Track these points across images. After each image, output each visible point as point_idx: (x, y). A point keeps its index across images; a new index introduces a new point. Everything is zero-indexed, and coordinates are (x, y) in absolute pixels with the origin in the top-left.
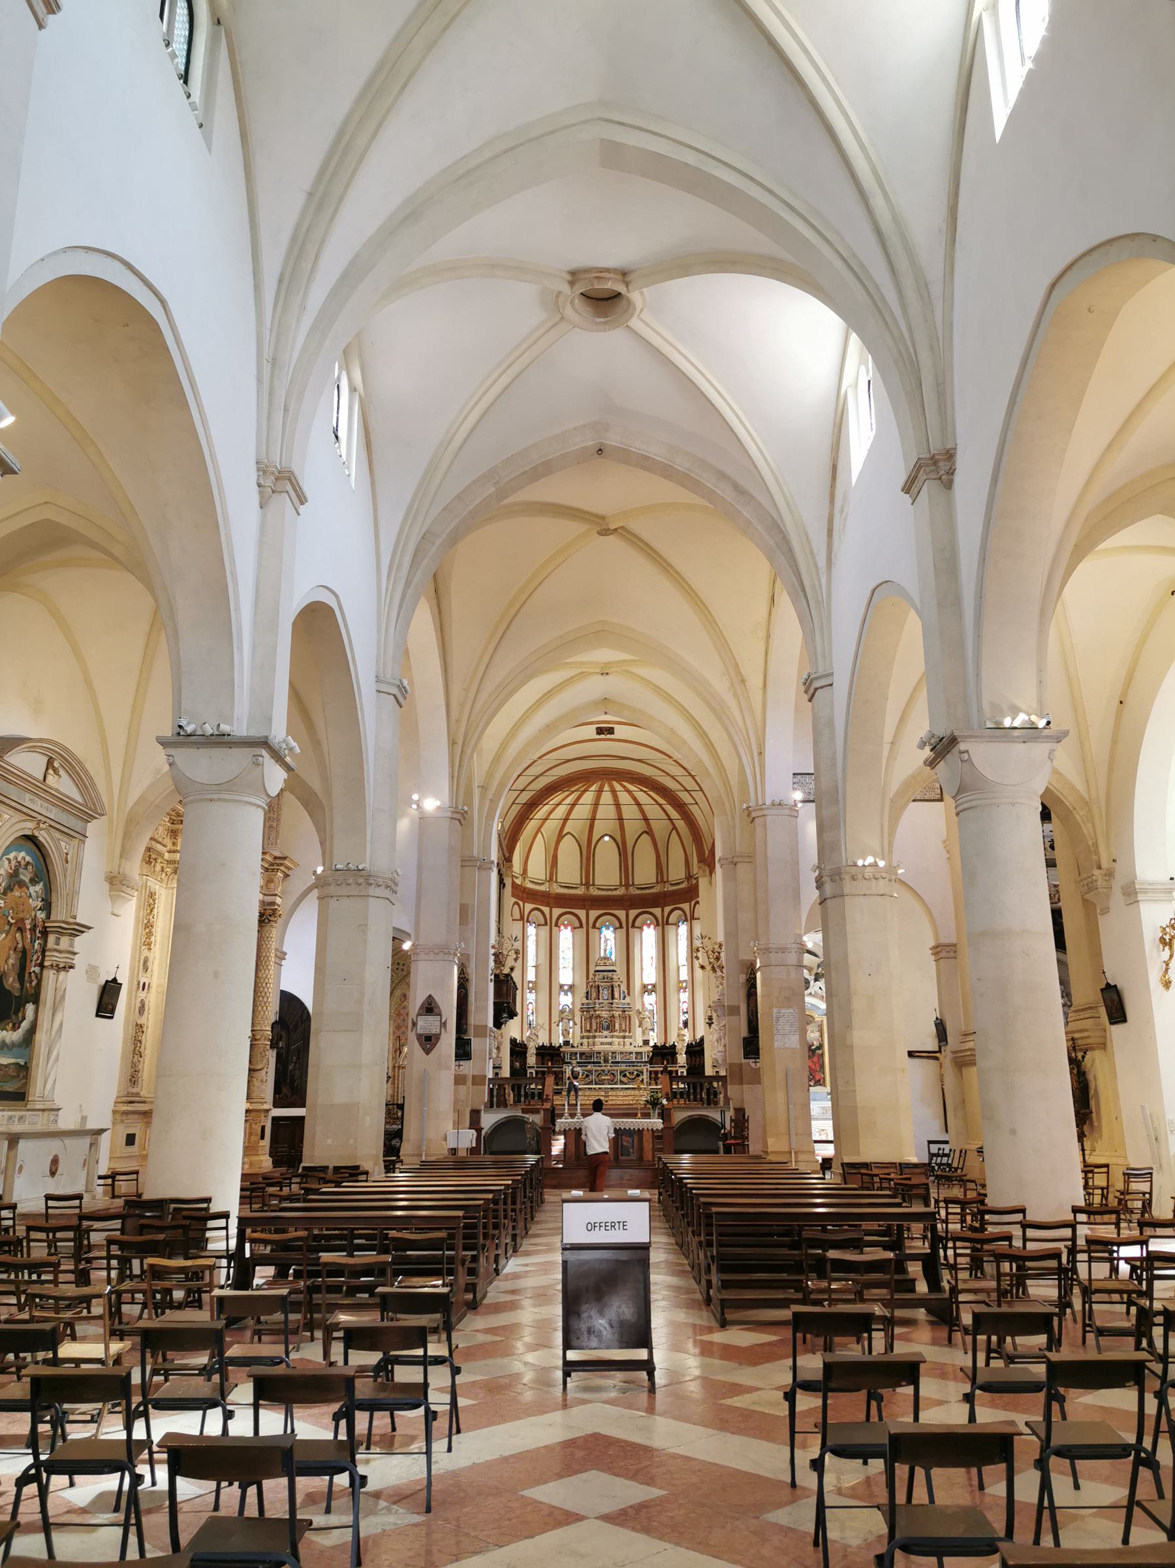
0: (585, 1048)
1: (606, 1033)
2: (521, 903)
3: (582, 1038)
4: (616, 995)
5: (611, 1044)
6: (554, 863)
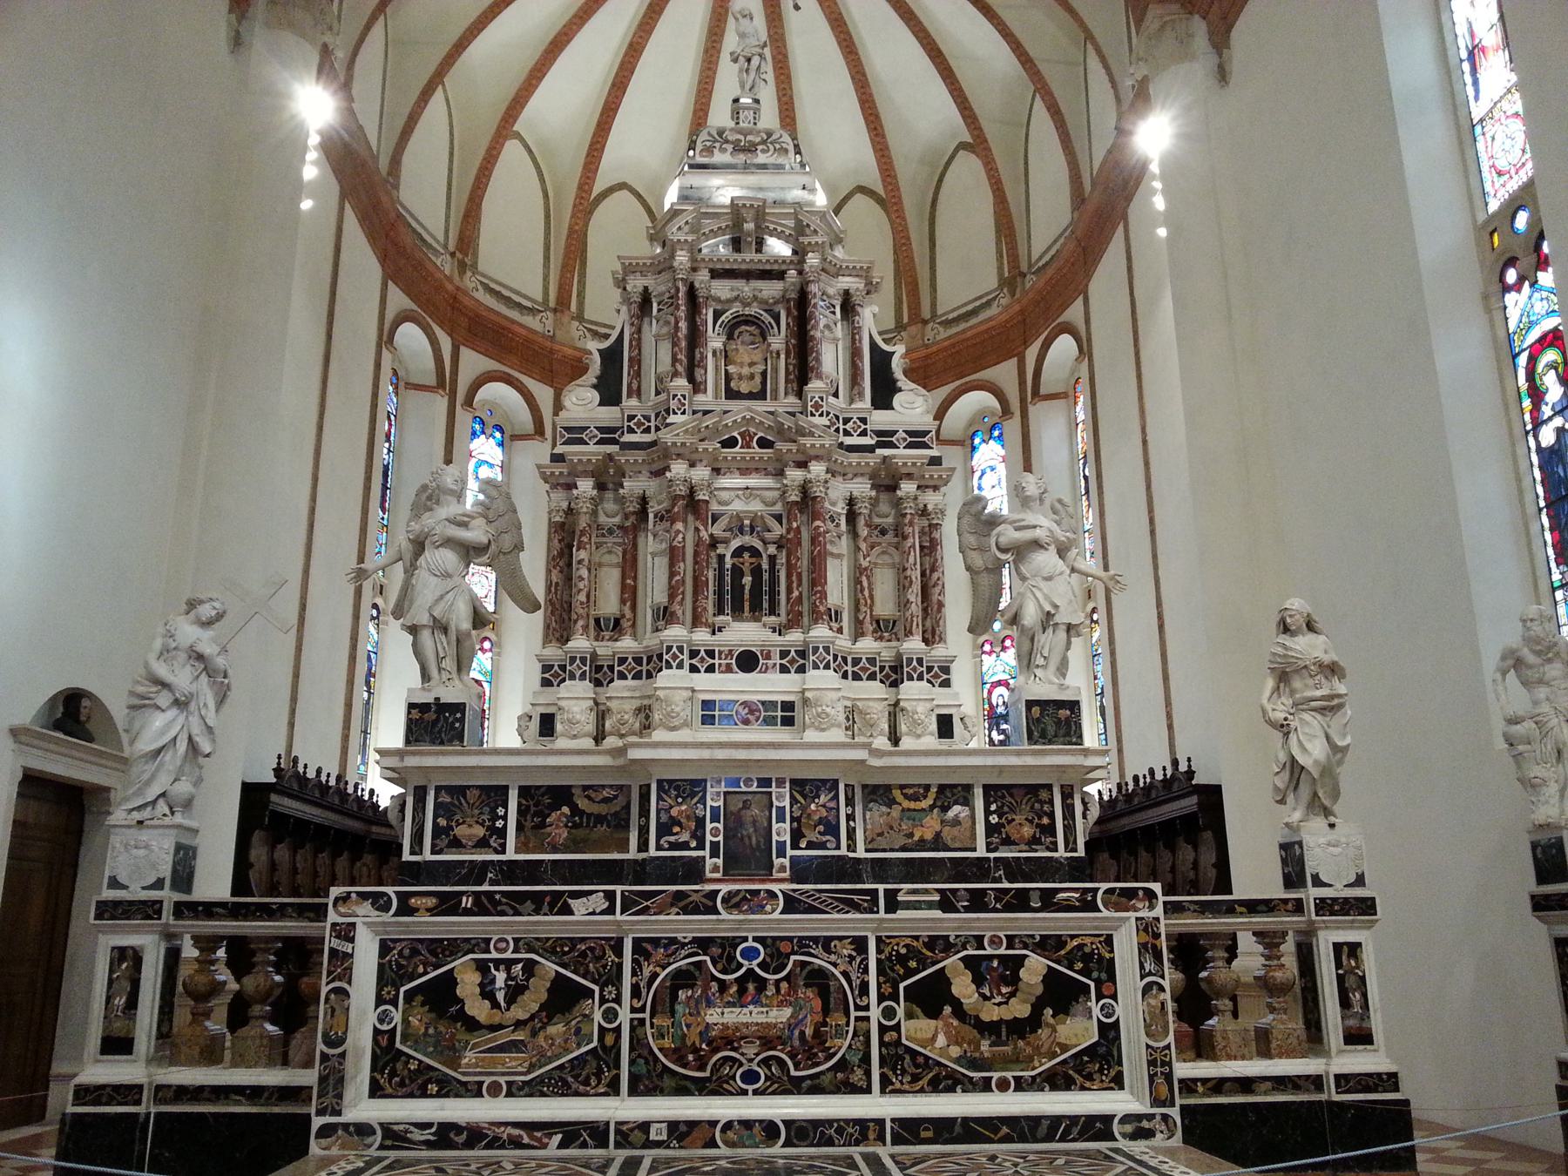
0: (573, 753)
1: (745, 633)
3: (551, 675)
4: (831, 358)
5: (787, 714)
6: (573, 254)
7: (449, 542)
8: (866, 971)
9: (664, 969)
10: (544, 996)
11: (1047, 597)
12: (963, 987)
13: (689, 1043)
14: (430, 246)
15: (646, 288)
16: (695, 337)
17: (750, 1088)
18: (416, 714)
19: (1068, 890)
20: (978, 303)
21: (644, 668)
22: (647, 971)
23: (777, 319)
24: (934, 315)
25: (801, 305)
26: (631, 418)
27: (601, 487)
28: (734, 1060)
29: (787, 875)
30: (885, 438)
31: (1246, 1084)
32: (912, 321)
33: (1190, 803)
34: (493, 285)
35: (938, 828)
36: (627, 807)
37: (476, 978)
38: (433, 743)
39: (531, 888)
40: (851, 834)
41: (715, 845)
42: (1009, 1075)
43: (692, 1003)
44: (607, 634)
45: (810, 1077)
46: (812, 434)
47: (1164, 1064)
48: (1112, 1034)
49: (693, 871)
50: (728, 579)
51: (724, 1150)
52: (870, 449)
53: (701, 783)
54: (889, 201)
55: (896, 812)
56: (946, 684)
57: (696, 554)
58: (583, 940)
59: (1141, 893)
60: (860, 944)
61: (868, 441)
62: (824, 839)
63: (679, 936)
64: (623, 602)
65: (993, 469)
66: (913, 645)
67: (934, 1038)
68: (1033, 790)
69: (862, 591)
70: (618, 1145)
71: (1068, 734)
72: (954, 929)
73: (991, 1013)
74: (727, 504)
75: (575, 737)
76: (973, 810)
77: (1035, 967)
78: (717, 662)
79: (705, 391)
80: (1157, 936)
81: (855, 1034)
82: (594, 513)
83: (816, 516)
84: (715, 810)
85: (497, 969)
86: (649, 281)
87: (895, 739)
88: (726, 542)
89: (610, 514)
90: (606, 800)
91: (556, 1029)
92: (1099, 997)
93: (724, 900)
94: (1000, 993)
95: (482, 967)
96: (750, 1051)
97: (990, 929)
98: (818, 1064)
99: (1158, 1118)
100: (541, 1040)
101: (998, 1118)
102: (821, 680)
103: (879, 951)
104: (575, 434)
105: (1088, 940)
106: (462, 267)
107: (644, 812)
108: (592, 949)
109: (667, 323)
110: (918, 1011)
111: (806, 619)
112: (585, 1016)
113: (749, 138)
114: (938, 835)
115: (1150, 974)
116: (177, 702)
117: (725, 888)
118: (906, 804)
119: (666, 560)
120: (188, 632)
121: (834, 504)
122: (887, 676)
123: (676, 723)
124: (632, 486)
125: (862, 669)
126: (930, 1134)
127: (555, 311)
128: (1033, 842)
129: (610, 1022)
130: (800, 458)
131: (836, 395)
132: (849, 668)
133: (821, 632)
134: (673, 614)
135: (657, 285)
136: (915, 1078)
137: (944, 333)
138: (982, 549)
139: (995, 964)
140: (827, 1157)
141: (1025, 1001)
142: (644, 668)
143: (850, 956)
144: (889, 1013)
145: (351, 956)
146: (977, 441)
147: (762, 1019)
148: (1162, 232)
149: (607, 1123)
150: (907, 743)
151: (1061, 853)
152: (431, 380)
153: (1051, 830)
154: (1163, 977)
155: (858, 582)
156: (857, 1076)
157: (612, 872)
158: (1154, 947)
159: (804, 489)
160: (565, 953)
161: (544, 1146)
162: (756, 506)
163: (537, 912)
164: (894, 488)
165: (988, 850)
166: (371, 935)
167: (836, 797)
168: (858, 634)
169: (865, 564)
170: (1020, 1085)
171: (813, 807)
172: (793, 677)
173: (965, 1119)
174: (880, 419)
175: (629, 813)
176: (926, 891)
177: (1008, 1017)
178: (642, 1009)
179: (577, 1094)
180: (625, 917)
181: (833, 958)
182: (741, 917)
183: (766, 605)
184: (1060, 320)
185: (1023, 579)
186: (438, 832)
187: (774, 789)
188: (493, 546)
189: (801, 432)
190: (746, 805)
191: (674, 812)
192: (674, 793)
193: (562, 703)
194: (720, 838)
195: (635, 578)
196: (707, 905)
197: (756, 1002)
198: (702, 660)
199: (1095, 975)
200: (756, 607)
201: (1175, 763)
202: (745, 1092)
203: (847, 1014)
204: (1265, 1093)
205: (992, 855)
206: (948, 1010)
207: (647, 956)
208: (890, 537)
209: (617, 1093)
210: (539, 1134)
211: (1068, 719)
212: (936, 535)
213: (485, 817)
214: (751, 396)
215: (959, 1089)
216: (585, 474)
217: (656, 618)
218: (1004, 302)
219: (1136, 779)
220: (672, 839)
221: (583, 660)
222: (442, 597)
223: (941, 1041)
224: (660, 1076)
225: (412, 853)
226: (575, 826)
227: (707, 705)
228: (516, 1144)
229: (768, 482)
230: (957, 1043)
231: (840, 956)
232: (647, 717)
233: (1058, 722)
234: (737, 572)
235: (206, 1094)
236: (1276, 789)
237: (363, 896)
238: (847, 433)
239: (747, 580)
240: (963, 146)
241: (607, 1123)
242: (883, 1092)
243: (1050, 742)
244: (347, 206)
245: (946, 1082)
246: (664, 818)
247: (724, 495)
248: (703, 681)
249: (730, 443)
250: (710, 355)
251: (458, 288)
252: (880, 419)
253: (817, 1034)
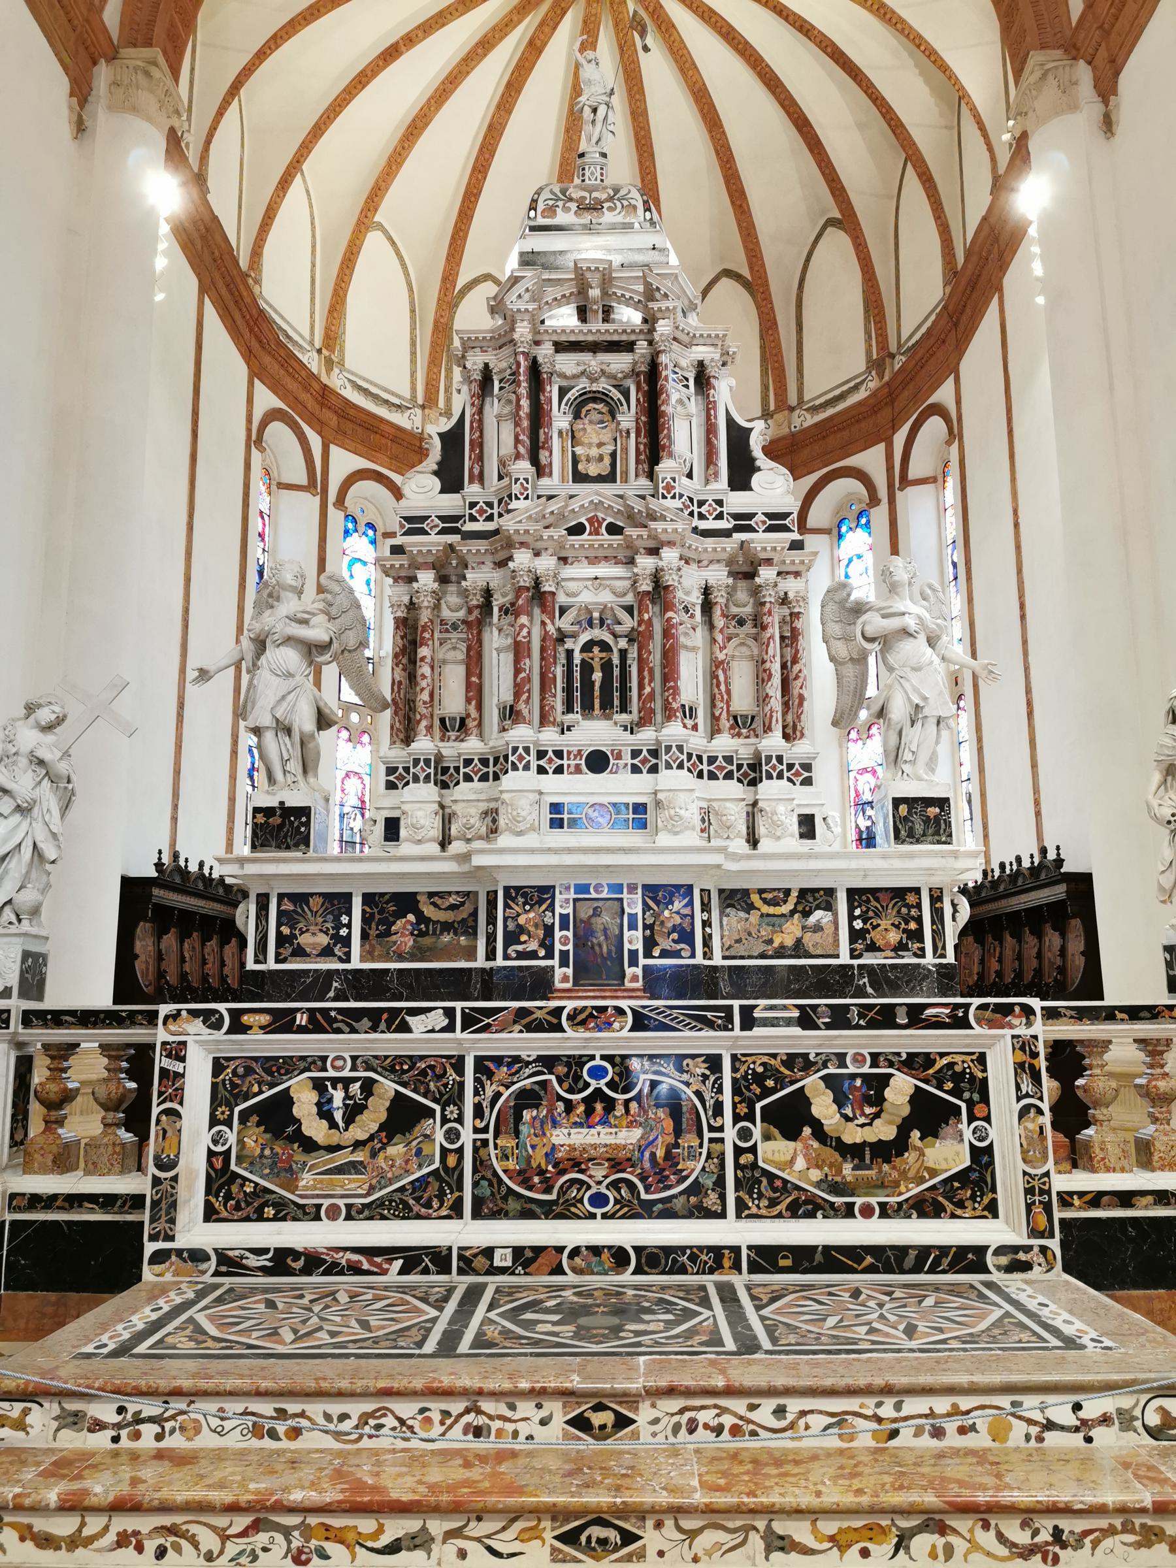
1: (594, 732)
2: (315, 441)
3: (395, 778)
7: (289, 640)
8: (720, 1091)
9: (507, 1087)
10: (383, 1116)
11: (916, 690)
12: (823, 1107)
13: (534, 1165)
14: (295, 343)
15: (486, 365)
16: (538, 417)
17: (599, 1212)
18: (261, 819)
19: (938, 1004)
20: (845, 388)
21: (491, 769)
22: (490, 1090)
23: (626, 394)
24: (801, 401)
26: (473, 505)
27: (443, 580)
28: (581, 1183)
29: (639, 984)
30: (743, 523)
31: (1125, 1198)
32: (778, 409)
33: (1058, 892)
34: (360, 382)
35: (799, 934)
36: (474, 914)
37: (313, 1097)
38: (279, 847)
39: (378, 997)
40: (707, 941)
41: (564, 955)
42: (873, 1201)
43: (537, 1124)
44: (453, 734)
45: (661, 1201)
46: (664, 518)
47: (1042, 1192)
48: (985, 1159)
49: (540, 984)
50: (577, 675)
51: (571, 1278)
52: (727, 533)
53: (550, 889)
54: (756, 285)
55: (754, 917)
56: (808, 782)
57: (543, 649)
58: (422, 1058)
59: (1017, 1009)
60: (714, 1063)
62: (679, 947)
63: (523, 1054)
64: (468, 700)
65: (859, 557)
66: (773, 743)
67: (792, 1161)
68: (899, 894)
69: (718, 685)
70: (461, 1271)
71: (937, 833)
72: (814, 1047)
73: (853, 1135)
74: (575, 595)
75: (419, 842)
76: (836, 915)
77: (901, 1087)
78: (565, 762)
79: (550, 474)
80: (1035, 1055)
81: (709, 1156)
82: (437, 607)
83: (667, 606)
84: (564, 919)
85: (335, 1088)
86: (490, 358)
87: (753, 841)
88: (574, 636)
89: (453, 609)
90: (453, 907)
91: (396, 1150)
92: (972, 1118)
93: (570, 1018)
94: (863, 1114)
95: (319, 1086)
96: (598, 1172)
97: (852, 1046)
98: (669, 1187)
99: (1036, 1250)
100: (380, 1160)
101: (861, 1247)
102: (673, 780)
103: (735, 1070)
104: (415, 524)
105: (958, 1059)
106: (329, 364)
107: (491, 920)
108: (432, 1067)
109: (509, 401)
110: (776, 1132)
111: (659, 717)
112: (426, 1136)
113: (594, 195)
114: (799, 942)
115: (1027, 1095)
116: (19, 809)
117: (570, 1005)
118: (766, 909)
119: (511, 656)
120: (29, 738)
121: (687, 593)
122: (745, 775)
123: (522, 827)
124: (476, 578)
125: (718, 768)
126: (788, 1263)
127: (423, 407)
128: (900, 947)
129: (453, 1143)
130: (651, 544)
131: (690, 476)
132: (705, 767)
133: (674, 731)
134: (519, 713)
135: (499, 362)
136: (773, 1203)
137: (810, 420)
138: (847, 639)
139: (858, 1082)
140: (680, 1287)
141: (890, 1123)
142: (491, 769)
143: (703, 1075)
144: (745, 1134)
145: (183, 1075)
146: (844, 529)
147: (610, 1140)
148: (1040, 300)
149: (450, 1249)
150: (765, 845)
151: (929, 960)
152: (303, 480)
153: (918, 935)
154: (1041, 1099)
155: (714, 676)
156: (711, 1200)
157: (454, 984)
158: (1032, 1066)
159: (656, 577)
160: (404, 1072)
161: (385, 1272)
162: (606, 597)
163: (374, 1029)
164: (751, 575)
165: (852, 957)
166: (203, 1053)
167: (691, 903)
168: (714, 731)
169: (721, 657)
170: (885, 1212)
171: (666, 913)
172: (645, 777)
173: (827, 1249)
174: (738, 501)
175: (476, 921)
176: (785, 1008)
177: (872, 1139)
178: (485, 1130)
179: (419, 1217)
180: (465, 1035)
181: (685, 1077)
182: (588, 1035)
183: (616, 702)
184: (930, 401)
185: (891, 669)
186: (281, 940)
188: (335, 645)
189: (653, 517)
190: (596, 912)
191: (522, 920)
192: (521, 900)
193: (405, 807)
194: (570, 947)
195: (480, 676)
197: (604, 1122)
198: (550, 761)
199: (966, 1095)
200: (606, 705)
201: (1043, 851)
202: (593, 1216)
203: (700, 1135)
204: (1146, 1207)
205: (856, 962)
206: (807, 1131)
207: (490, 1075)
208: (748, 628)
209: (460, 1216)
210: (378, 1260)
211: (937, 818)
212: (798, 624)
213: (329, 925)
214: (600, 479)
215: (819, 1214)
217: (503, 717)
218: (872, 385)
219: (1002, 866)
220: (520, 948)
221: (427, 762)
222: (283, 698)
223: (800, 1164)
224: (505, 1199)
225: (257, 962)
226: (422, 934)
227: (556, 808)
228: (356, 1270)
229: (619, 571)
230: (818, 1167)
231: (693, 1075)
232: (494, 821)
233: (927, 821)
234: (587, 668)
235: (59, 1203)
236: (1161, 889)
237: (194, 1013)
238: (702, 517)
239: (597, 676)
240: (831, 222)
241: (450, 1249)
242: (739, 1216)
243: (918, 841)
244: (207, 300)
245: (804, 1207)
246: (511, 926)
247: (571, 586)
248: (550, 782)
249: (577, 530)
250: (555, 436)
251: (325, 387)
252: (738, 501)
253: (668, 1156)
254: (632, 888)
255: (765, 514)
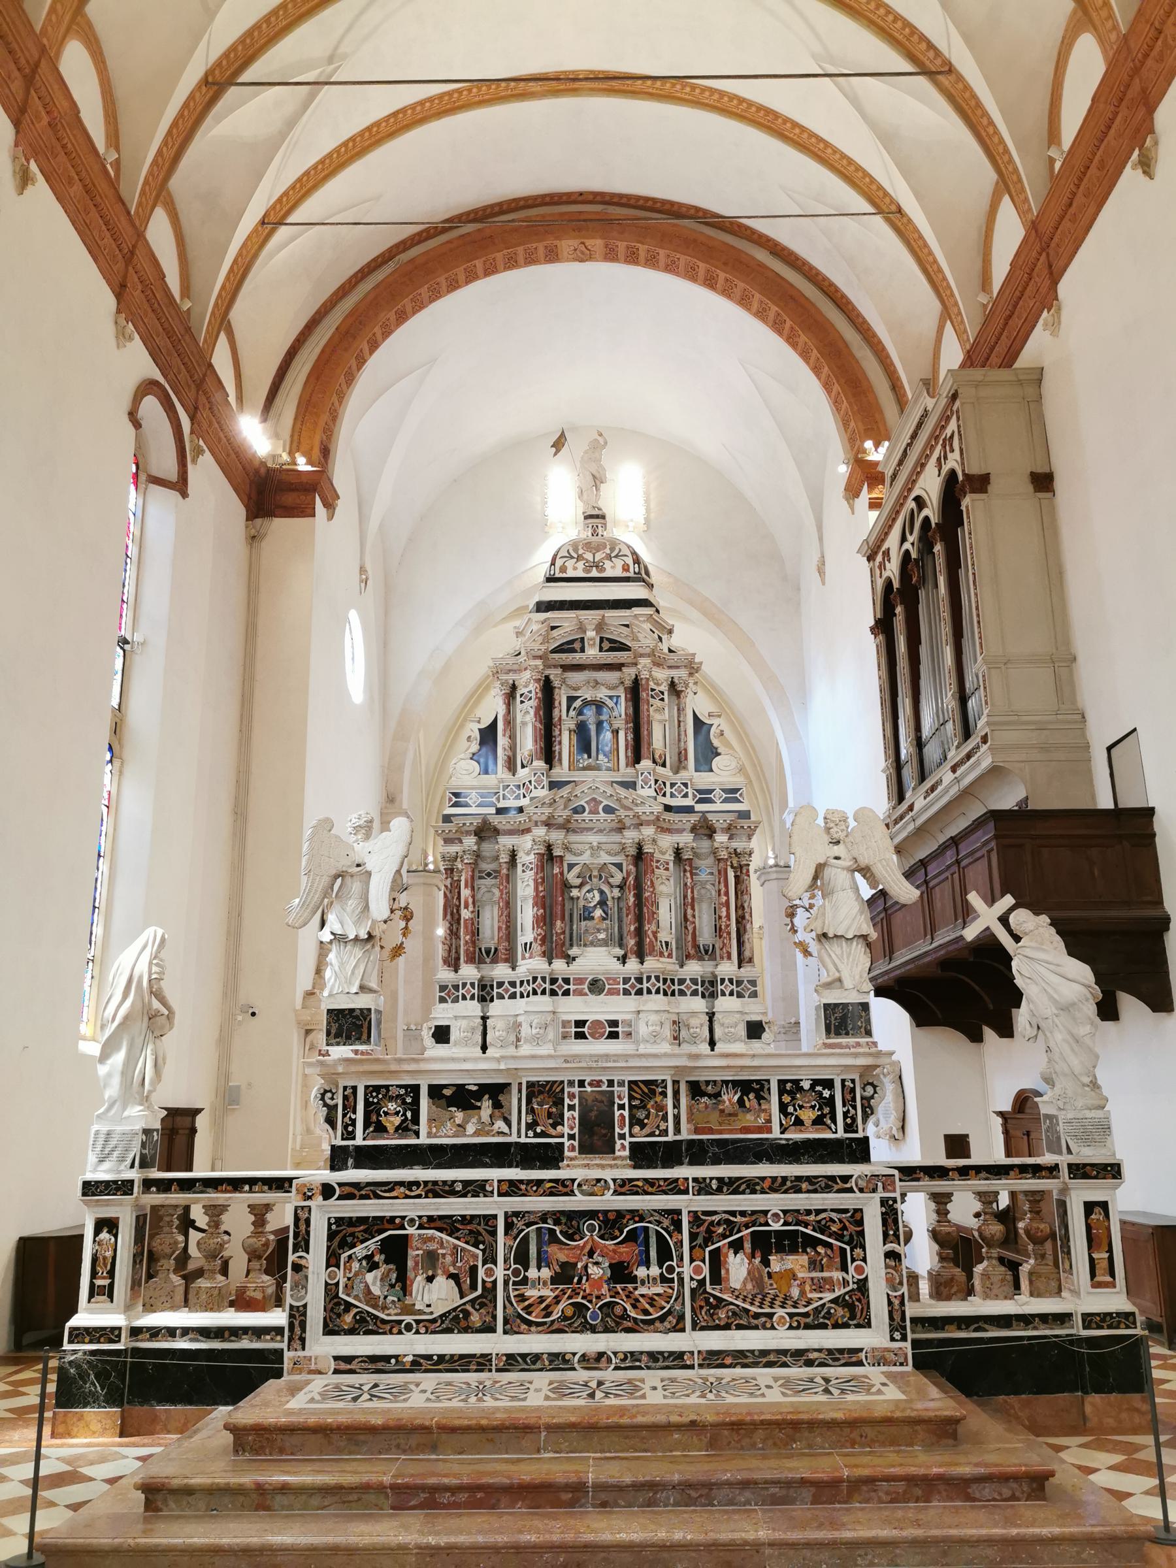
25: (635, 691)
30: (705, 796)
56: (754, 995)
61: (688, 802)
66: (727, 968)
87: (712, 1044)
131: (664, 765)
133: (652, 964)
150: (719, 1047)
187: (616, 1088)
196: (562, 1188)
216: (468, 833)
221: (472, 985)
252: (703, 780)
254: (621, 1084)
255: (723, 790)
